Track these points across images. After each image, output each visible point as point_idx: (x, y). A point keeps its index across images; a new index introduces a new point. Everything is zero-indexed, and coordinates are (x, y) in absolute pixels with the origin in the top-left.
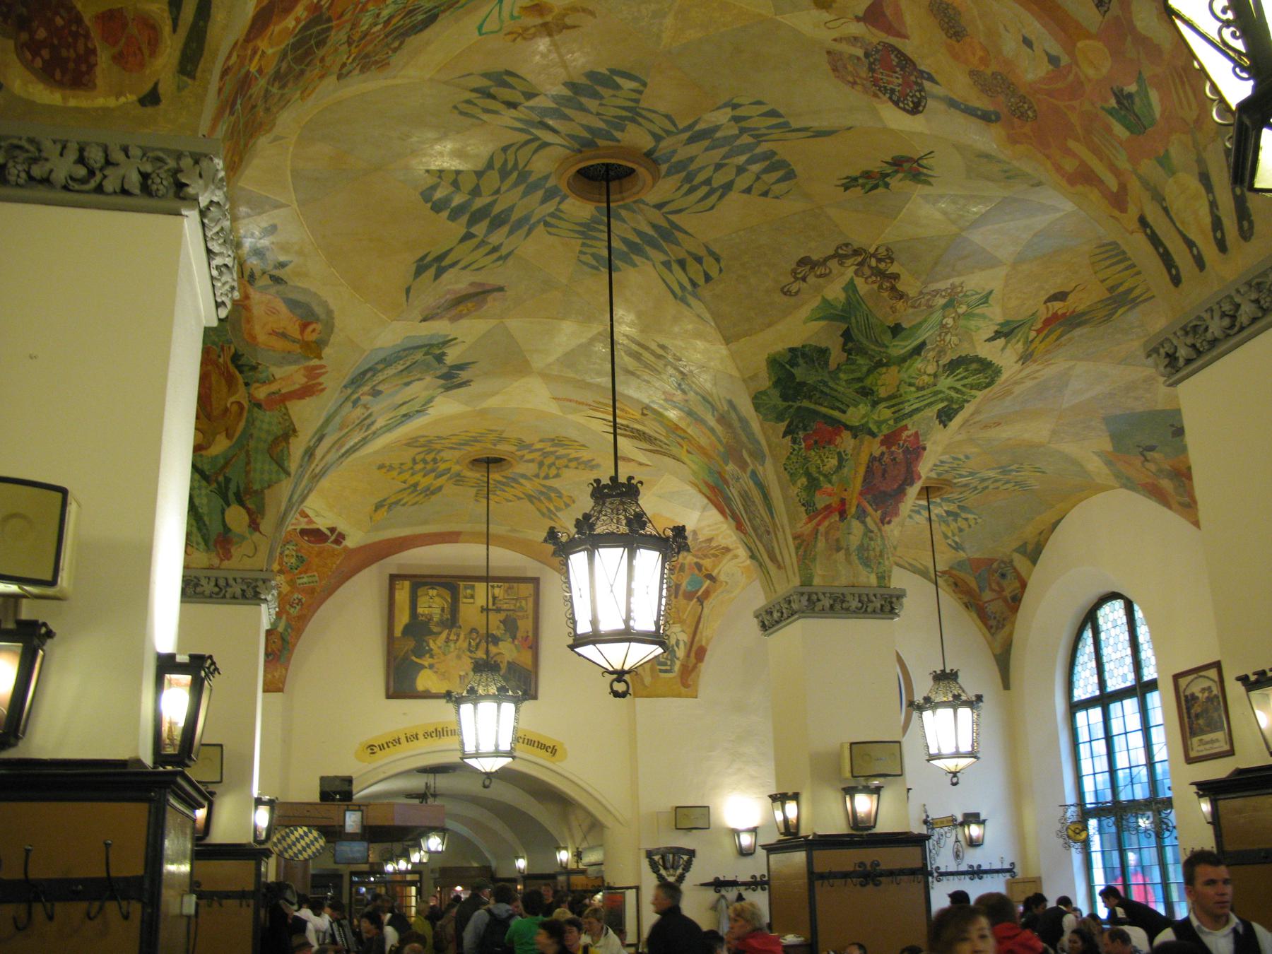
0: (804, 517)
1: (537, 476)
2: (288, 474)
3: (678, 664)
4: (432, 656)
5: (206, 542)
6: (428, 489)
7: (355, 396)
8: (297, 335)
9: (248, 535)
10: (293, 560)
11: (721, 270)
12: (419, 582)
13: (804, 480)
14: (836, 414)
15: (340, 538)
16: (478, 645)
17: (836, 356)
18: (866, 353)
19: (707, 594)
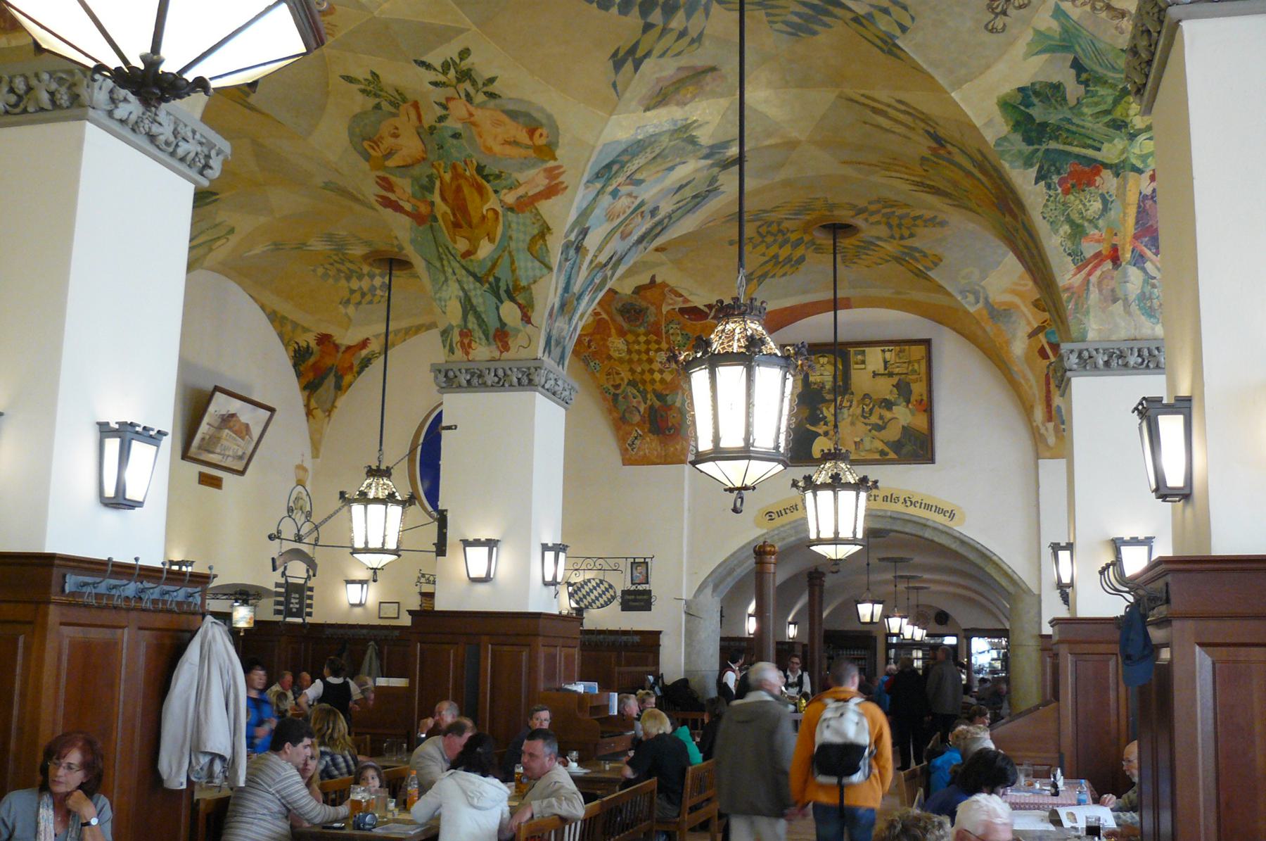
0: (1072, 267)
2: (550, 269)
4: (826, 424)
5: (487, 339)
7: (610, 189)
8: (527, 141)
11: (913, 19)
12: (816, 349)
13: (1067, 228)
14: (1090, 153)
16: (871, 410)
17: (1073, 90)
18: (1106, 82)
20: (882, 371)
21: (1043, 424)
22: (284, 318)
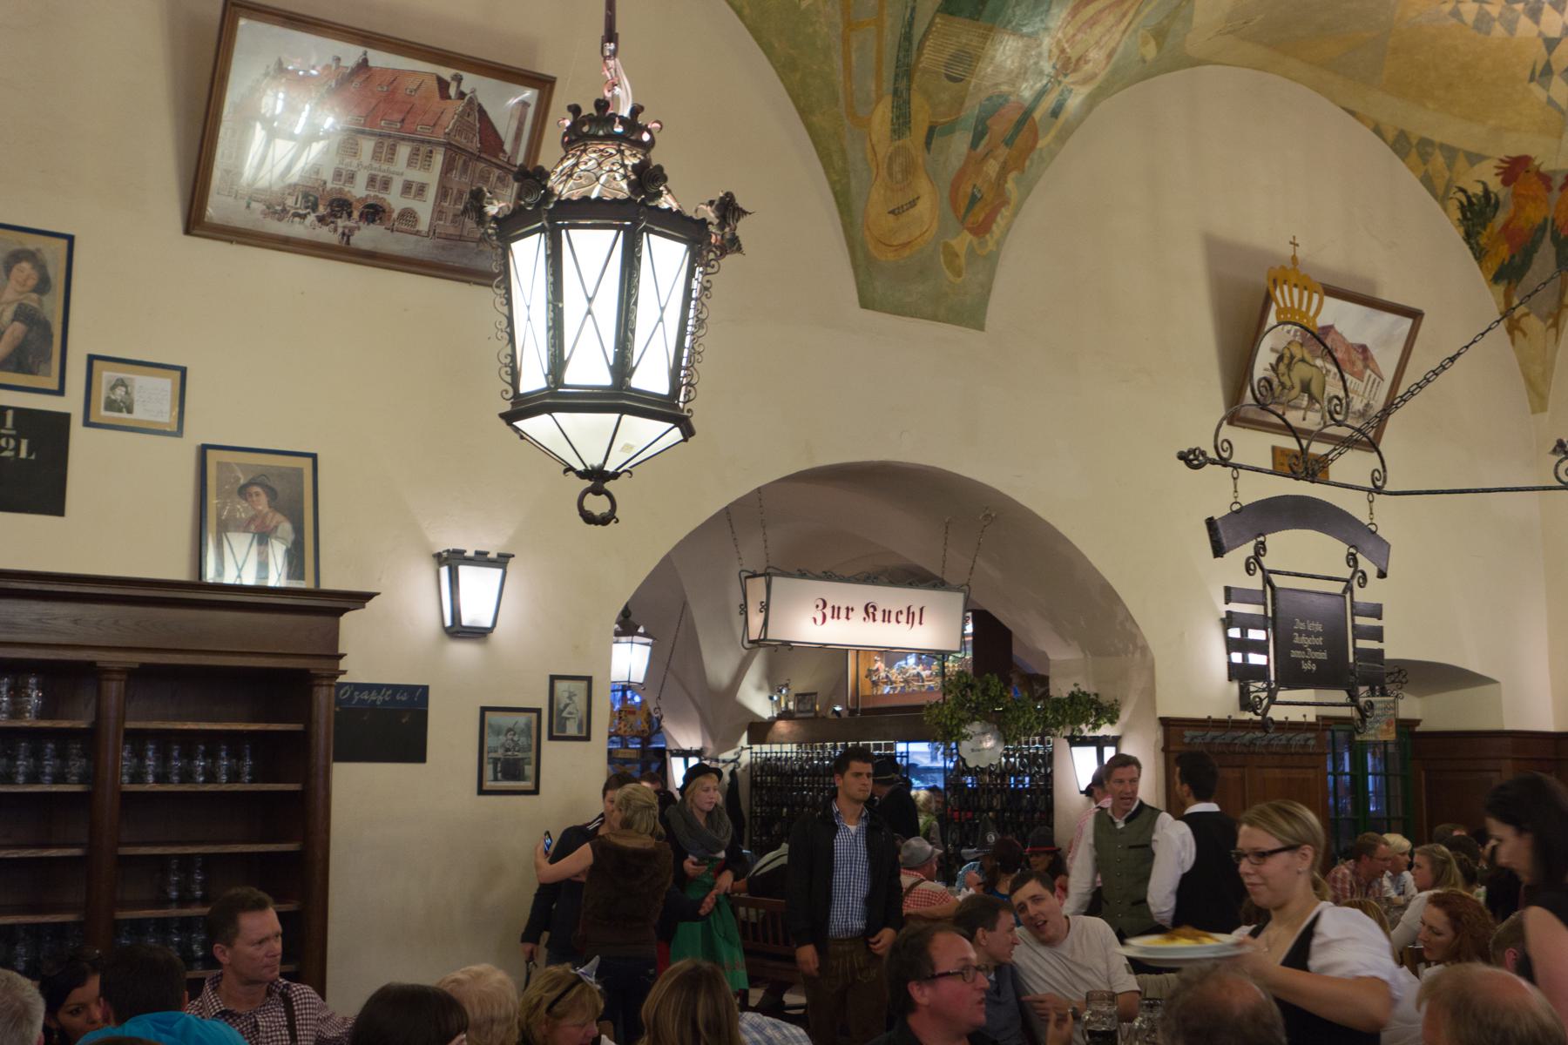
22: (1425, 143)
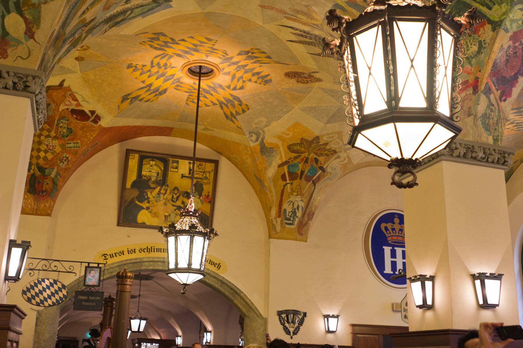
1: (229, 87)
3: (297, 220)
4: (148, 202)
6: (158, 90)
9: (24, 41)
10: (65, 131)
12: (144, 157)
15: (97, 119)
16: (178, 198)
19: (319, 179)
20: (187, 175)
21: (275, 219)
